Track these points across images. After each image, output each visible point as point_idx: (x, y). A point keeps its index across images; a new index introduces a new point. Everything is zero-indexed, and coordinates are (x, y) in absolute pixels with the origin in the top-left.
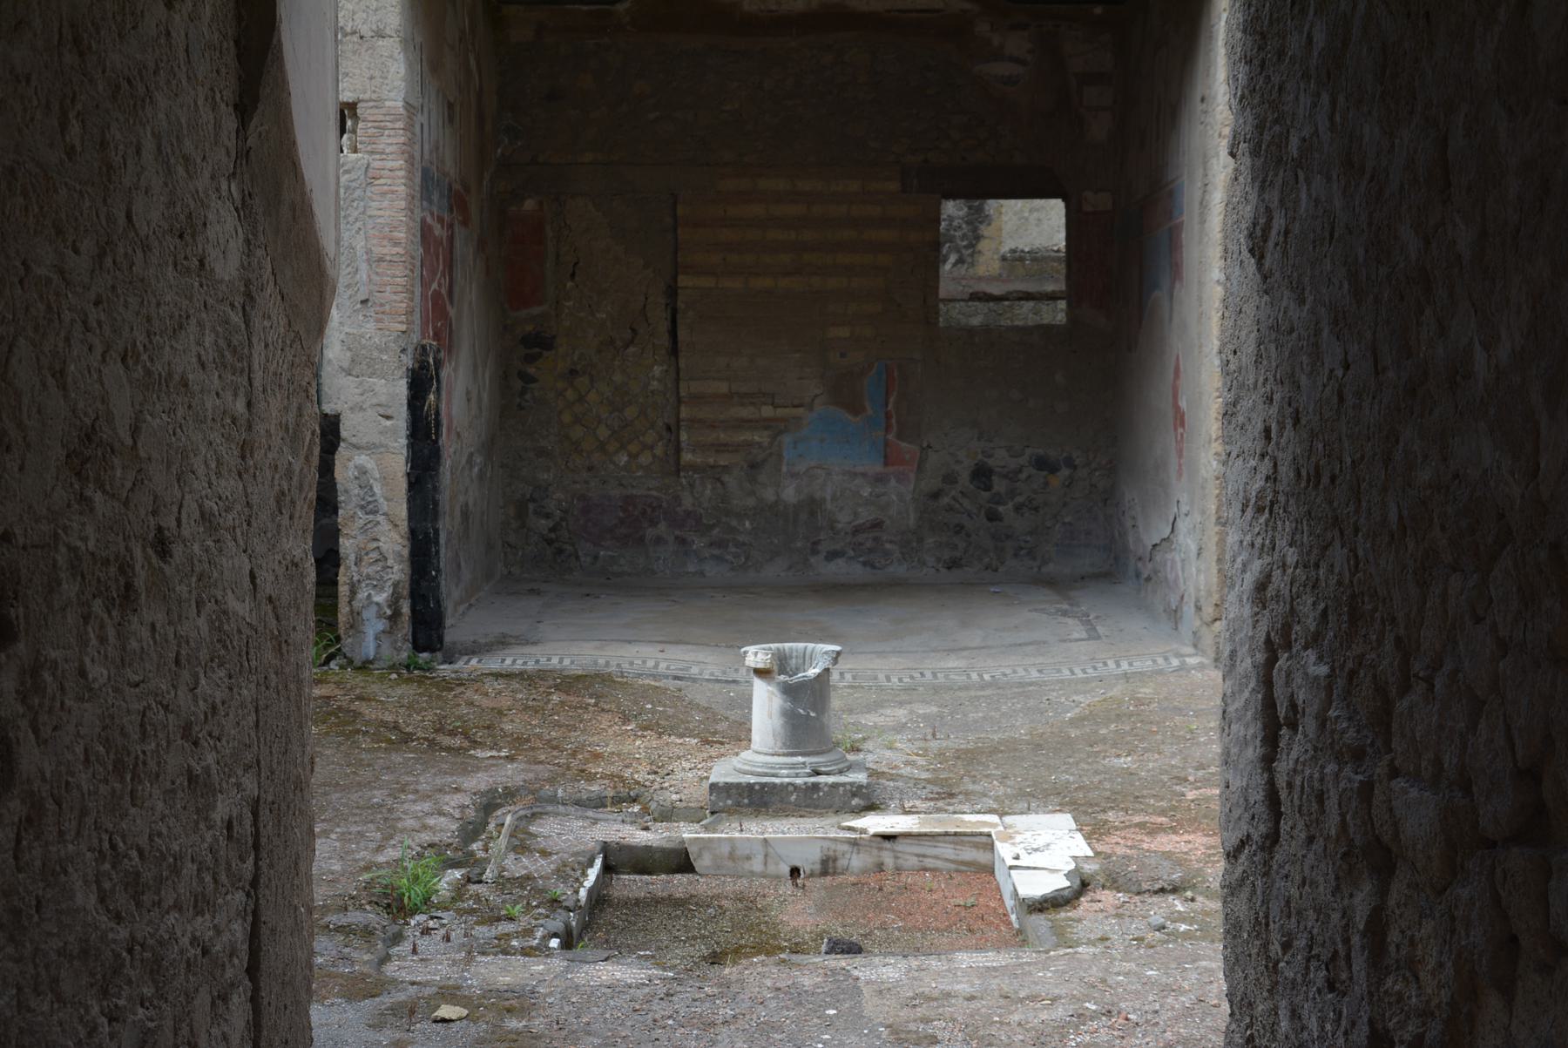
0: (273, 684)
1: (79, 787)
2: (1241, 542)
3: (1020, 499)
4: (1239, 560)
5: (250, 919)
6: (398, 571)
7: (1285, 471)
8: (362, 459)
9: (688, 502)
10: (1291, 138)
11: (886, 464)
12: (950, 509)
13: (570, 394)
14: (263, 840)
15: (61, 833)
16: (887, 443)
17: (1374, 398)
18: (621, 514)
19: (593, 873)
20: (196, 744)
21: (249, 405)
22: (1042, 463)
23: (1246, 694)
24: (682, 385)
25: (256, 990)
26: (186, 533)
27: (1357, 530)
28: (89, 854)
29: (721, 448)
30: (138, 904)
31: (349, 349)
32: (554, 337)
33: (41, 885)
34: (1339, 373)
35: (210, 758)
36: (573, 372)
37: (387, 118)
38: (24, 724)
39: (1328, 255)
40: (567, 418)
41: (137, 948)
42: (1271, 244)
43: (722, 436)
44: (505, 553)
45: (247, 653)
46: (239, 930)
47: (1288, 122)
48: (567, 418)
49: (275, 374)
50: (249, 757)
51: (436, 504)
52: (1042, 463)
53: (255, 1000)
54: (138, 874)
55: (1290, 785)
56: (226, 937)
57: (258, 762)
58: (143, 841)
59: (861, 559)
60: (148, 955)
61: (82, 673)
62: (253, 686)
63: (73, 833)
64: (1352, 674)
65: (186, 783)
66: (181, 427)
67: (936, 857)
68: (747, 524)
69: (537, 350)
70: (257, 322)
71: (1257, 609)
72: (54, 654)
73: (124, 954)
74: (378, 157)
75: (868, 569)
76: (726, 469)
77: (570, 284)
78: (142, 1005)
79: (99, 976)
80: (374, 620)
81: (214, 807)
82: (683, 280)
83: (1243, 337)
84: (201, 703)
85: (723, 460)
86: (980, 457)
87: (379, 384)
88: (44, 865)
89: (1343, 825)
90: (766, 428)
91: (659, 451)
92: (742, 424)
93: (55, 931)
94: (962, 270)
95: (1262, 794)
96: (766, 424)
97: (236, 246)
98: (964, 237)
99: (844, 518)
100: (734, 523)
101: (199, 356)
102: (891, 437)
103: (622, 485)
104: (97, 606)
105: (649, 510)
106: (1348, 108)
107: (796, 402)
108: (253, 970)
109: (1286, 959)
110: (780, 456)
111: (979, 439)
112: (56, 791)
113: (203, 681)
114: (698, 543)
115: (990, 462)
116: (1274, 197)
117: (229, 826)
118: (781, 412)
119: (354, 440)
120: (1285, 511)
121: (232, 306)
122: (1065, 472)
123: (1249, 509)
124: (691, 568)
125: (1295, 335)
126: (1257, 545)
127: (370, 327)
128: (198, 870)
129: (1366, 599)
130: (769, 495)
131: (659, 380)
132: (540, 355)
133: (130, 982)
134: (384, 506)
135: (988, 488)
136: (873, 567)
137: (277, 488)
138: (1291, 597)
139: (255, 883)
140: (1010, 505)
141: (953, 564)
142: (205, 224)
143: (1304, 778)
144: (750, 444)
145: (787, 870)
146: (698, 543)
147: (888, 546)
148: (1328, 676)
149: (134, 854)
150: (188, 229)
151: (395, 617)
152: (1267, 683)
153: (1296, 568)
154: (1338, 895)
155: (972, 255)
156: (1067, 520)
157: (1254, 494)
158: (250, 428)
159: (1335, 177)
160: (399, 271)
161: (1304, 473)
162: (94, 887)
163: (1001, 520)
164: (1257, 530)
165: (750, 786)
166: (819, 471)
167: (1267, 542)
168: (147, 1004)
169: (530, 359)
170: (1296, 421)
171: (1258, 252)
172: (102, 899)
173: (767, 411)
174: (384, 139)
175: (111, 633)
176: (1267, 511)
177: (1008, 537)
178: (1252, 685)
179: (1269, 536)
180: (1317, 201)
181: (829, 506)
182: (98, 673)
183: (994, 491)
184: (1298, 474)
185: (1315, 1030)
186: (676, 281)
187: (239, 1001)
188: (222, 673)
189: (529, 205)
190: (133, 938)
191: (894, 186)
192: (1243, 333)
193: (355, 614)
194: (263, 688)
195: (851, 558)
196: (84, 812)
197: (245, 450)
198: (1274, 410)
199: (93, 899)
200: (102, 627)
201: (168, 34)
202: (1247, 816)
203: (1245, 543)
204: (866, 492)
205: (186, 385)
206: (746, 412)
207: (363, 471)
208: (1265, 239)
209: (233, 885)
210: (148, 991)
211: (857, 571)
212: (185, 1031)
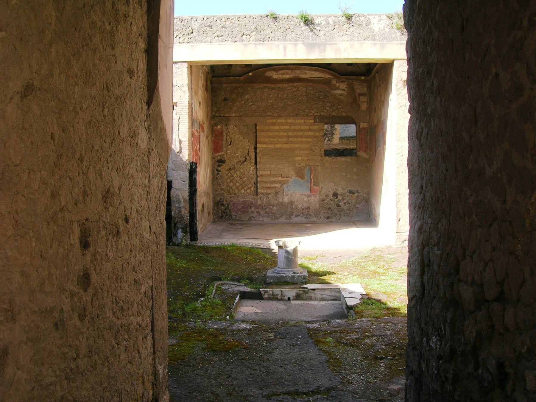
0: (156, 256)
1: (107, 285)
2: (414, 216)
3: (345, 201)
4: (414, 221)
5: (151, 317)
7: (428, 197)
9: (259, 202)
10: (428, 109)
11: (311, 192)
12: (327, 204)
13: (229, 174)
14: (154, 297)
15: (103, 297)
16: (311, 187)
17: (455, 179)
18: (243, 205)
19: (237, 299)
20: (136, 272)
21: (149, 181)
22: (351, 192)
23: (416, 257)
24: (258, 172)
25: (153, 335)
26: (133, 216)
27: (450, 215)
28: (110, 303)
29: (268, 188)
30: (123, 315)
31: (174, 164)
32: (226, 160)
33: (99, 311)
34: (445, 172)
35: (140, 276)
36: (230, 169)
37: (184, 106)
38: (92, 269)
39: (441, 140)
40: (228, 181)
41: (123, 326)
42: (423, 137)
43: (268, 185)
44: (213, 216)
45: (149, 248)
46: (148, 320)
47: (427, 105)
48: (228, 181)
49: (156, 173)
50: (150, 275)
51: (196, 203)
52: (351, 192)
53: (153, 338)
54: (122, 307)
55: (428, 282)
56: (145, 322)
57: (152, 276)
58: (123, 298)
59: (304, 217)
60: (126, 328)
61: (107, 255)
62: (150, 256)
63: (106, 297)
64: (448, 254)
65: (134, 283)
66: (131, 188)
67: (325, 295)
68: (275, 208)
69: (221, 164)
70: (151, 159)
71: (419, 235)
72: (99, 250)
73: (120, 328)
74: (182, 116)
75: (306, 219)
76: (269, 194)
77: (229, 147)
78: (125, 340)
79: (114, 334)
80: (181, 233)
81: (141, 289)
82: (258, 145)
83: (414, 161)
84: (137, 261)
86: (335, 190)
88: (99, 306)
89: (445, 294)
90: (280, 183)
91: (252, 189)
92: (274, 182)
93: (102, 323)
94: (329, 142)
95: (420, 284)
96: (280, 182)
97: (146, 139)
98: (329, 134)
99: (300, 206)
100: (271, 208)
101: (136, 168)
102: (312, 185)
103: (242, 198)
104: (110, 237)
105: (250, 204)
106: (446, 101)
107: (287, 176)
108: (152, 330)
109: (426, 328)
110: (284, 190)
111: (334, 186)
112: (101, 286)
113: (138, 256)
115: (337, 192)
116: (423, 125)
117: (145, 293)
119: (175, 187)
120: (428, 208)
121: (145, 155)
122: (356, 194)
123: (416, 208)
124: (260, 219)
125: (431, 161)
126: (419, 217)
128: (138, 305)
129: (453, 233)
130: (281, 200)
131: (252, 171)
132: (222, 165)
133: (122, 335)
135: (337, 198)
136: (308, 219)
137: (156, 203)
138: (430, 232)
139: (152, 308)
140: (343, 203)
141: (328, 218)
142: (138, 134)
143: (433, 281)
144: (276, 187)
146: (262, 212)
147: (311, 213)
148: (441, 254)
149: (121, 302)
150: (134, 135)
152: (421, 254)
153: (431, 224)
154: (442, 312)
155: (332, 138)
156: (357, 206)
157: (418, 203)
158: (149, 187)
159: (442, 119)
161: (434, 199)
162: (111, 311)
163: (340, 206)
164: (419, 213)
165: (277, 277)
166: (293, 194)
167: (422, 217)
168: (126, 340)
169: (219, 166)
170: (432, 185)
171: (419, 139)
172: (114, 314)
173: (280, 179)
174: (184, 111)
175: (114, 244)
176: (422, 208)
177: (342, 211)
178: (417, 255)
179: (422, 215)
180: (437, 125)
181: (296, 203)
182: (111, 255)
183: (338, 199)
184: (432, 199)
185: (434, 347)
186: (256, 145)
187: (149, 338)
188: (142, 253)
189: (219, 127)
190: (122, 323)
191: (312, 121)
192: (414, 160)
194: (153, 257)
195: (302, 216)
196: (108, 292)
197: (148, 193)
198: (424, 181)
199: (111, 314)
200: (111, 242)
201: (130, 85)
202: (415, 290)
203: (415, 217)
205: (133, 177)
208: (421, 136)
209: (147, 309)
210: (126, 337)
211: (303, 219)
212: (136, 347)
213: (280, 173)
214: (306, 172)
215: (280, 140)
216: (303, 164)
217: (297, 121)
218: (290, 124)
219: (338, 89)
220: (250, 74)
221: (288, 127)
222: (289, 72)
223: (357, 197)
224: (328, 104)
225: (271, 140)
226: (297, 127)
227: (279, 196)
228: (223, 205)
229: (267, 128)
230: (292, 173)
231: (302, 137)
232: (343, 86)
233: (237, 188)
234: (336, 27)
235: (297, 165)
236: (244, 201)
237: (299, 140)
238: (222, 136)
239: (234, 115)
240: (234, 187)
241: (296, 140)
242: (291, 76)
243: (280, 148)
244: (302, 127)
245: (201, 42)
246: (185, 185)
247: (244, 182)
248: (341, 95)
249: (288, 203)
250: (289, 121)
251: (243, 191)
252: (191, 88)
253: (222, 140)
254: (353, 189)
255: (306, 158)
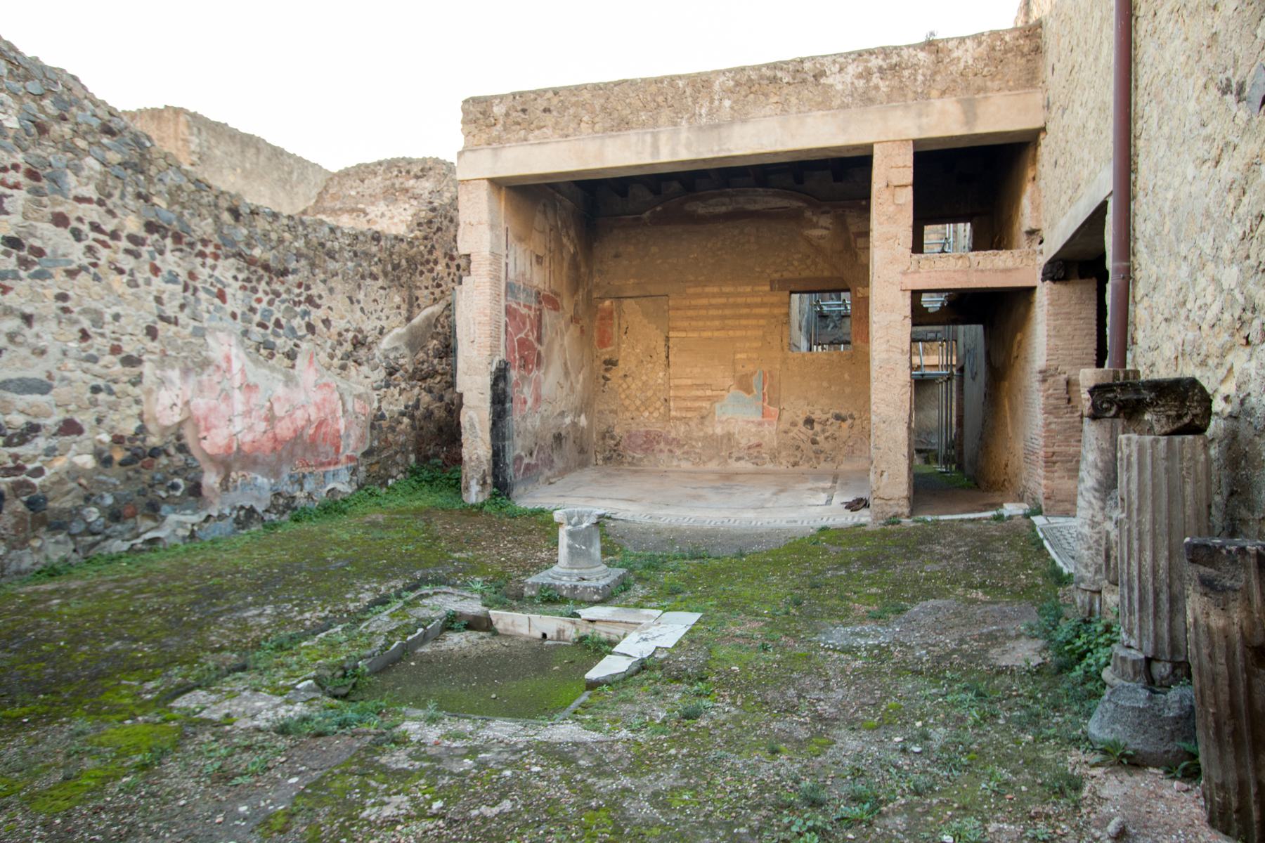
6: (486, 467)
8: (471, 413)
9: (673, 434)
13: (625, 386)
22: (838, 417)
29: (688, 409)
40: (623, 396)
48: (623, 396)
51: (504, 433)
52: (838, 417)
82: (672, 334)
85: (689, 415)
87: (478, 378)
91: (662, 410)
92: (698, 398)
96: (709, 398)
99: (744, 442)
114: (678, 452)
115: (813, 417)
118: (715, 393)
122: (849, 421)
127: (475, 353)
130: (710, 431)
134: (480, 434)
141: (795, 464)
144: (701, 408)
145: (539, 636)
151: (485, 483)
160: (487, 328)
169: (607, 370)
173: (709, 393)
189: (607, 303)
191: (767, 288)
193: (468, 482)
204: (754, 430)
206: (700, 393)
207: (471, 418)
213: (709, 382)
214: (756, 381)
215: (708, 323)
216: (749, 368)
217: (741, 289)
218: (727, 295)
219: (815, 226)
220: (659, 209)
221: (723, 300)
222: (727, 200)
223: (852, 427)
224: (796, 256)
225: (694, 323)
226: (740, 300)
227: (706, 423)
228: (612, 438)
229: (686, 302)
230: (729, 382)
231: (747, 317)
232: (825, 221)
233: (637, 409)
234: (753, 89)
235: (739, 367)
236: (648, 433)
237: (744, 322)
238: (611, 318)
239: (632, 281)
240: (632, 408)
241: (737, 322)
242: (730, 208)
243: (710, 339)
244: (749, 300)
245: (508, 140)
246: (484, 400)
247: (648, 399)
248: (822, 237)
249: (723, 437)
250: (727, 289)
251: (646, 414)
252: (493, 227)
253: (611, 325)
254: (844, 413)
255: (755, 356)
